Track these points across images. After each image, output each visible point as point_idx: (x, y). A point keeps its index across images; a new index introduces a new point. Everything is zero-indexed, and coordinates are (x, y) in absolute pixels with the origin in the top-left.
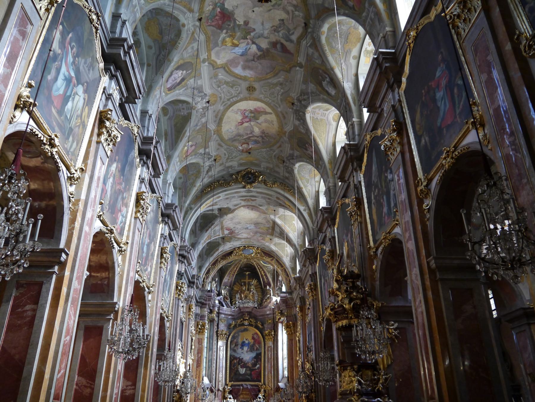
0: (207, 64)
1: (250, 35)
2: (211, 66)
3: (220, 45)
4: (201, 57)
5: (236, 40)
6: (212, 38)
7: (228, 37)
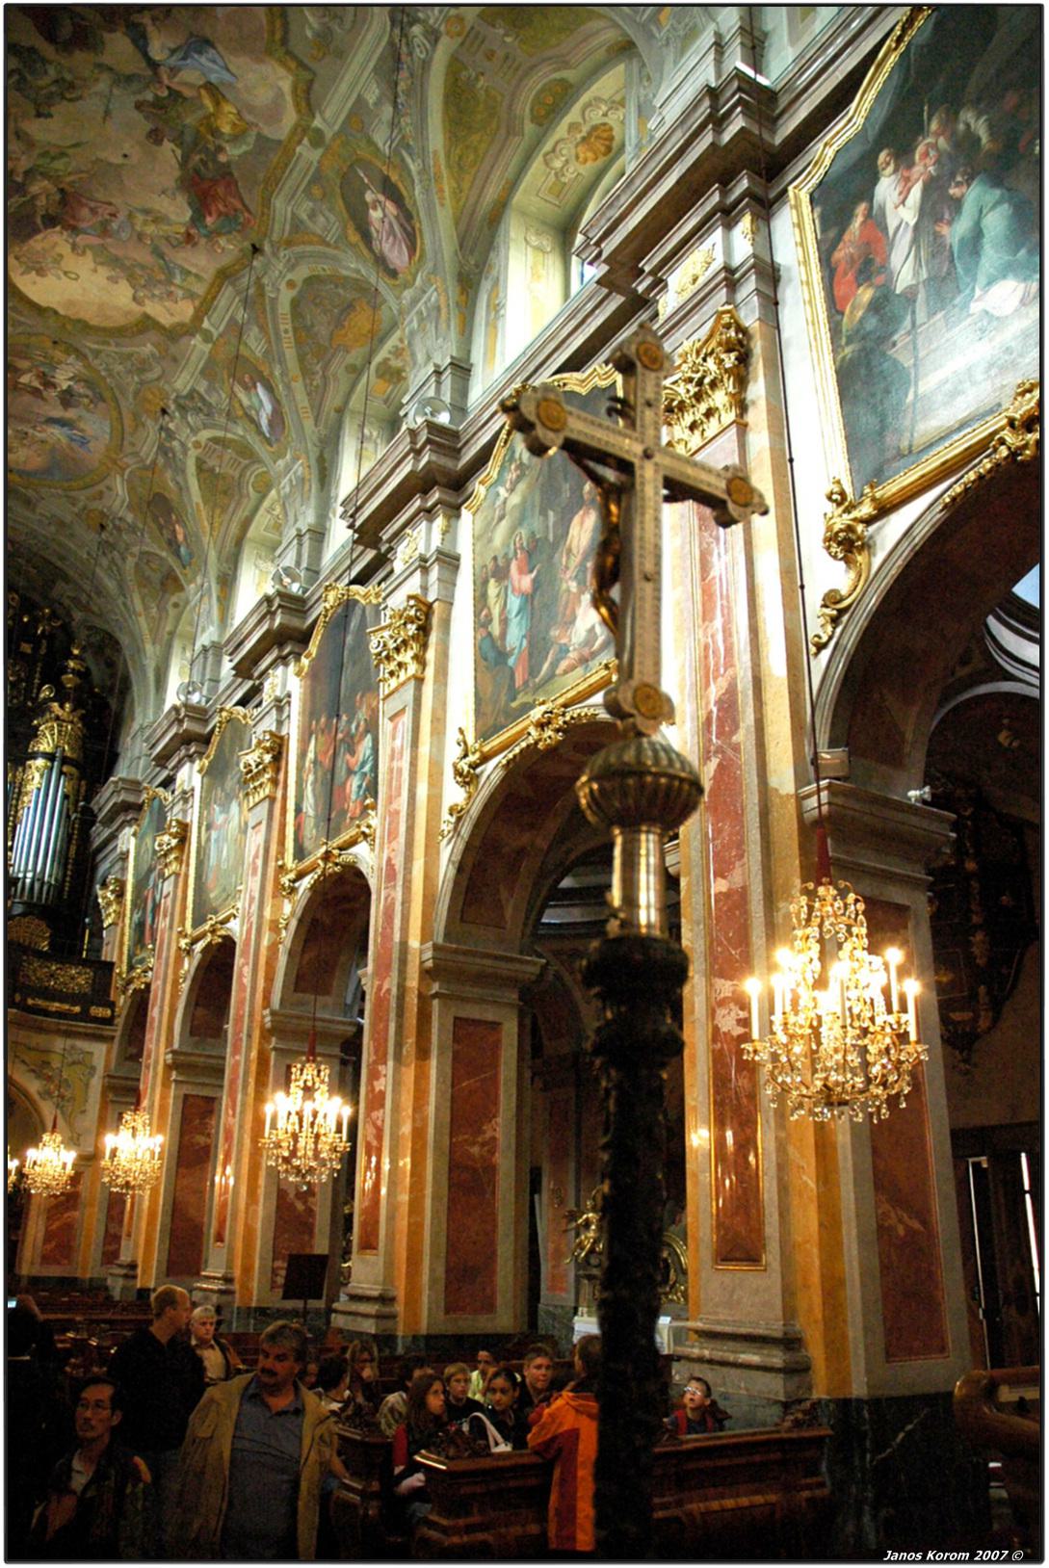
0: (317, 123)
1: (156, 96)
2: (313, 96)
3: (253, 133)
4: (315, 164)
5: (202, 106)
6: (261, 176)
7: (222, 134)
